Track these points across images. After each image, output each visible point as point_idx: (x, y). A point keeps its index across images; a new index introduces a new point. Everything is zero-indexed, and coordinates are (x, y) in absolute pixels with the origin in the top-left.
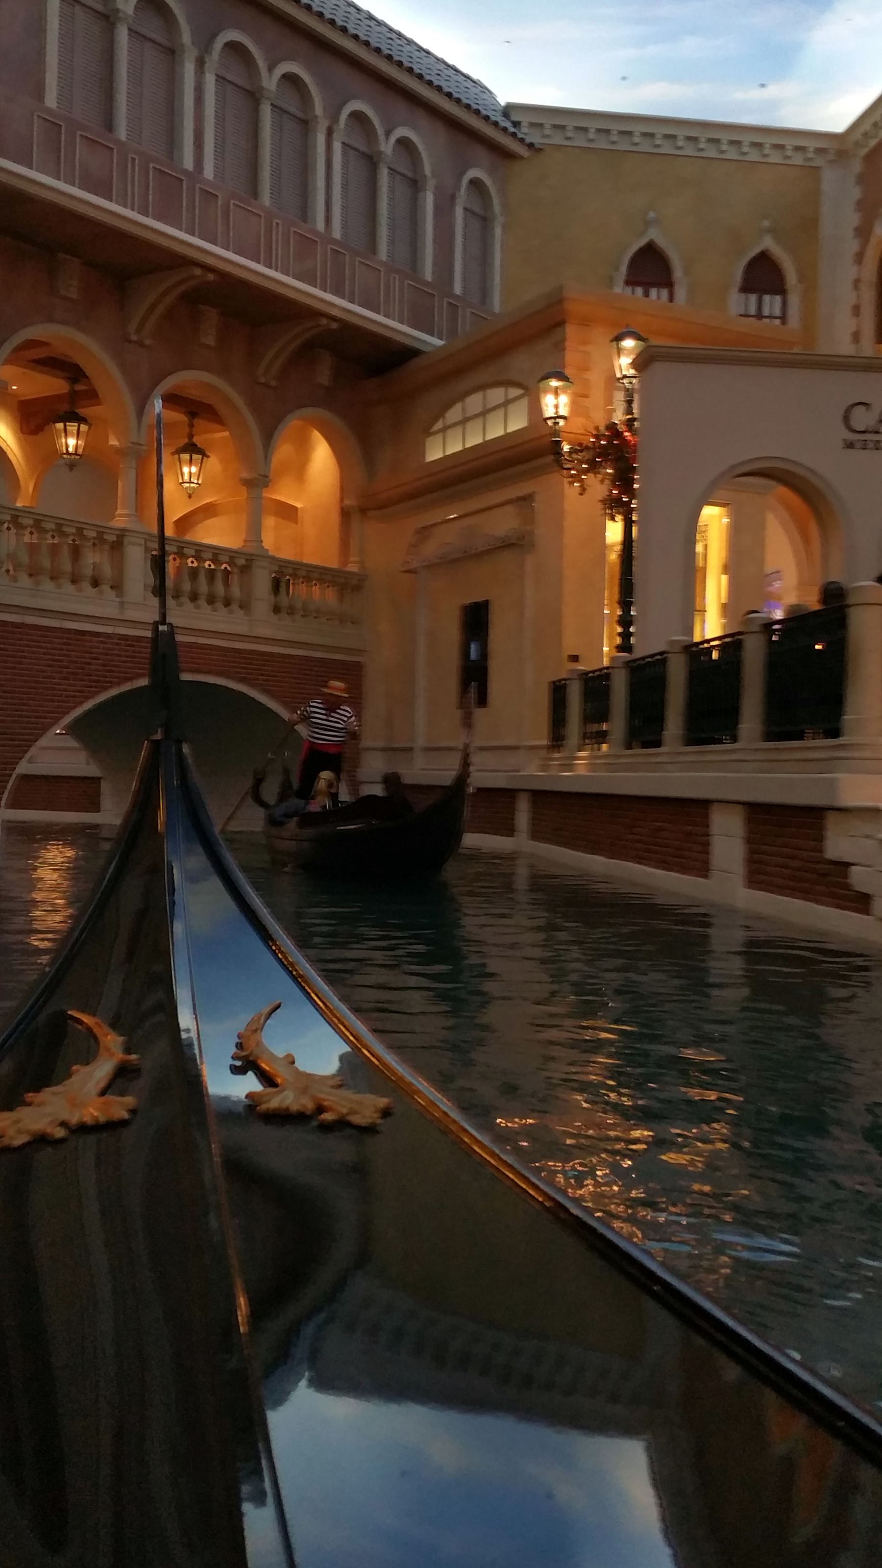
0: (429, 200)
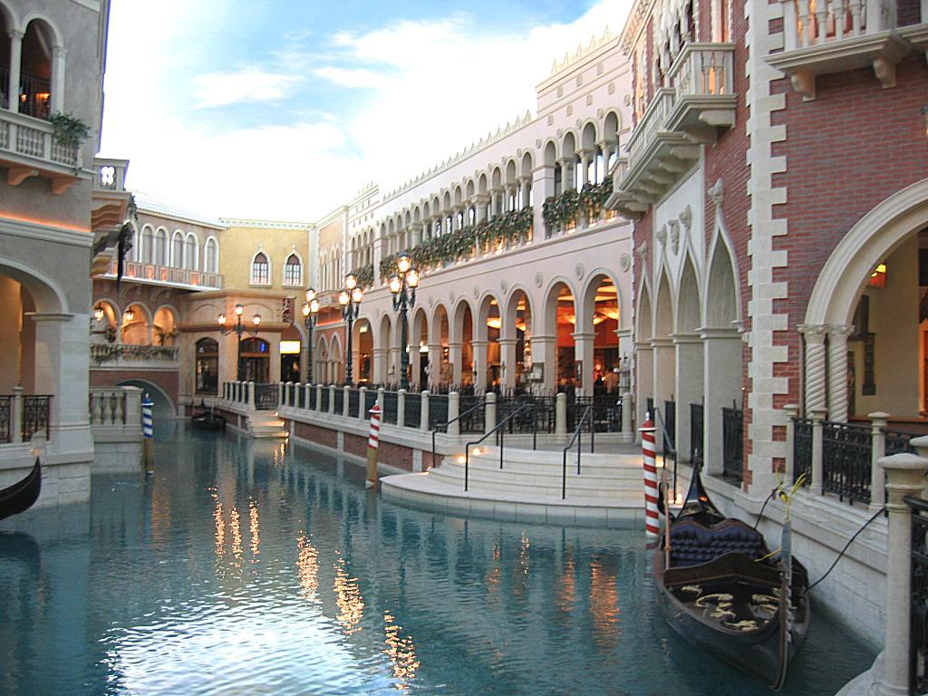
0: (197, 248)
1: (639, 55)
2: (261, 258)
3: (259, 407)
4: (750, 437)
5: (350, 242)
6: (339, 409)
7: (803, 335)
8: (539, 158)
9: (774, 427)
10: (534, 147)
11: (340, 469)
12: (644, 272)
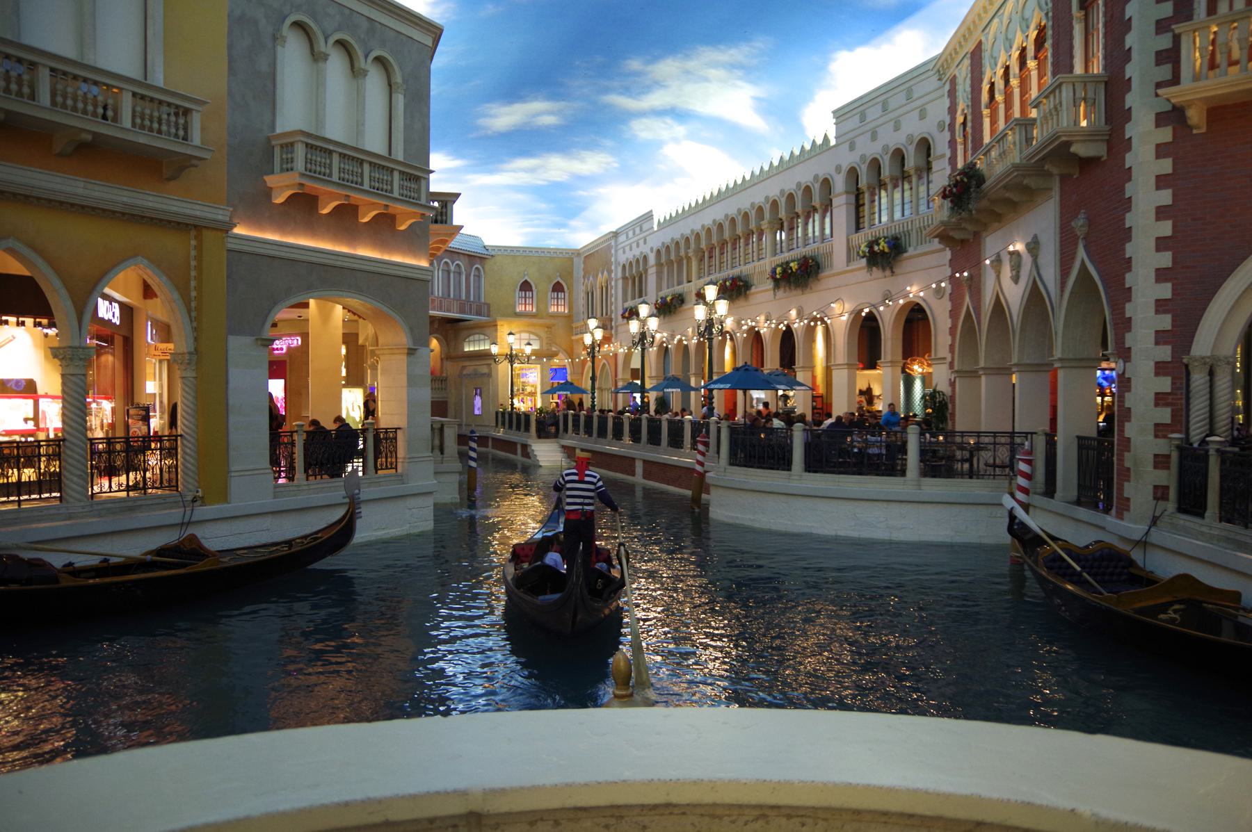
1: (960, 80)
2: (526, 286)
3: (539, 437)
4: (1127, 464)
5: (620, 269)
6: (636, 437)
7: (1187, 366)
8: (839, 184)
9: (1156, 456)
10: (833, 173)
11: (639, 493)
12: (967, 299)
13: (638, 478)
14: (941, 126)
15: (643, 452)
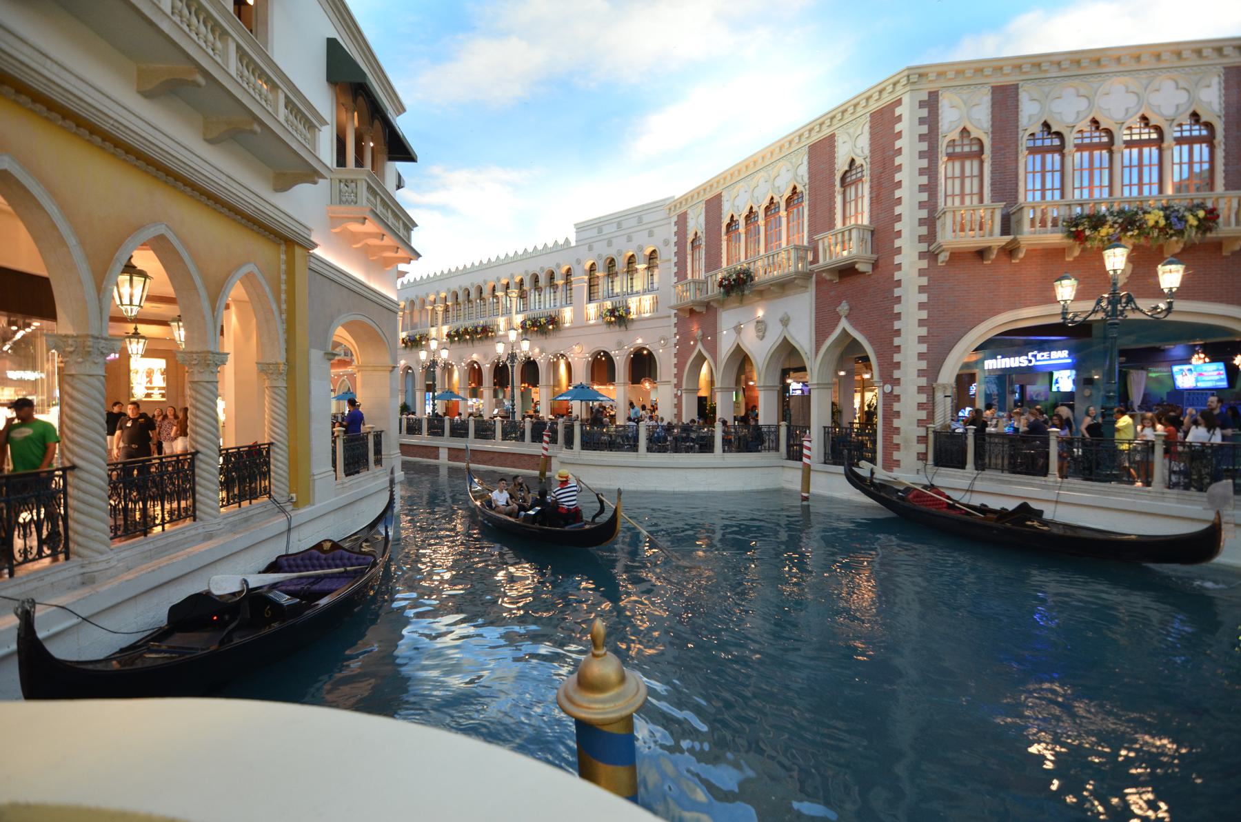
11: (443, 472)
13: (444, 458)
14: (666, 243)
15: (445, 443)
